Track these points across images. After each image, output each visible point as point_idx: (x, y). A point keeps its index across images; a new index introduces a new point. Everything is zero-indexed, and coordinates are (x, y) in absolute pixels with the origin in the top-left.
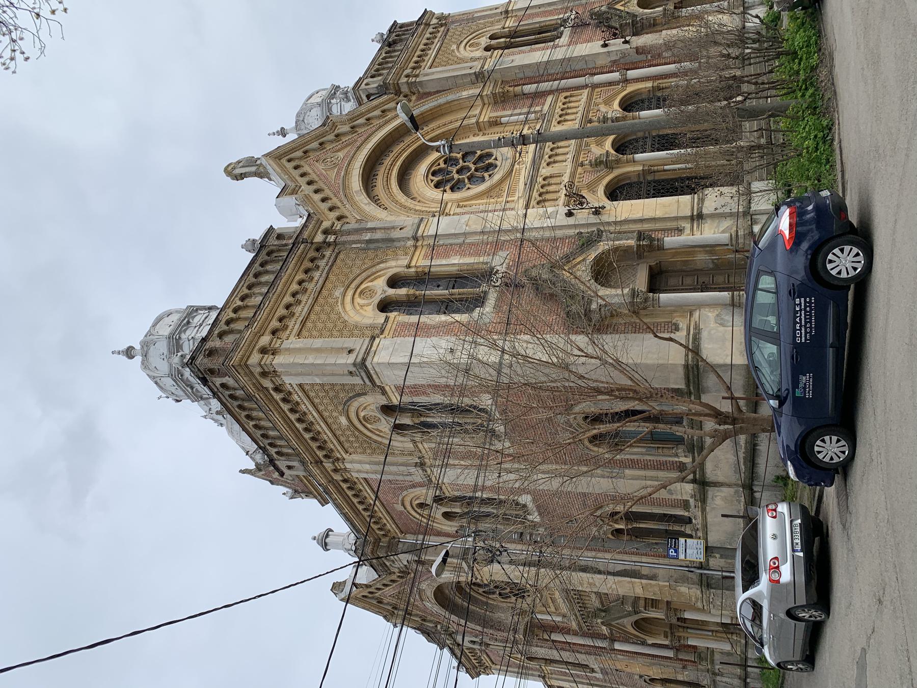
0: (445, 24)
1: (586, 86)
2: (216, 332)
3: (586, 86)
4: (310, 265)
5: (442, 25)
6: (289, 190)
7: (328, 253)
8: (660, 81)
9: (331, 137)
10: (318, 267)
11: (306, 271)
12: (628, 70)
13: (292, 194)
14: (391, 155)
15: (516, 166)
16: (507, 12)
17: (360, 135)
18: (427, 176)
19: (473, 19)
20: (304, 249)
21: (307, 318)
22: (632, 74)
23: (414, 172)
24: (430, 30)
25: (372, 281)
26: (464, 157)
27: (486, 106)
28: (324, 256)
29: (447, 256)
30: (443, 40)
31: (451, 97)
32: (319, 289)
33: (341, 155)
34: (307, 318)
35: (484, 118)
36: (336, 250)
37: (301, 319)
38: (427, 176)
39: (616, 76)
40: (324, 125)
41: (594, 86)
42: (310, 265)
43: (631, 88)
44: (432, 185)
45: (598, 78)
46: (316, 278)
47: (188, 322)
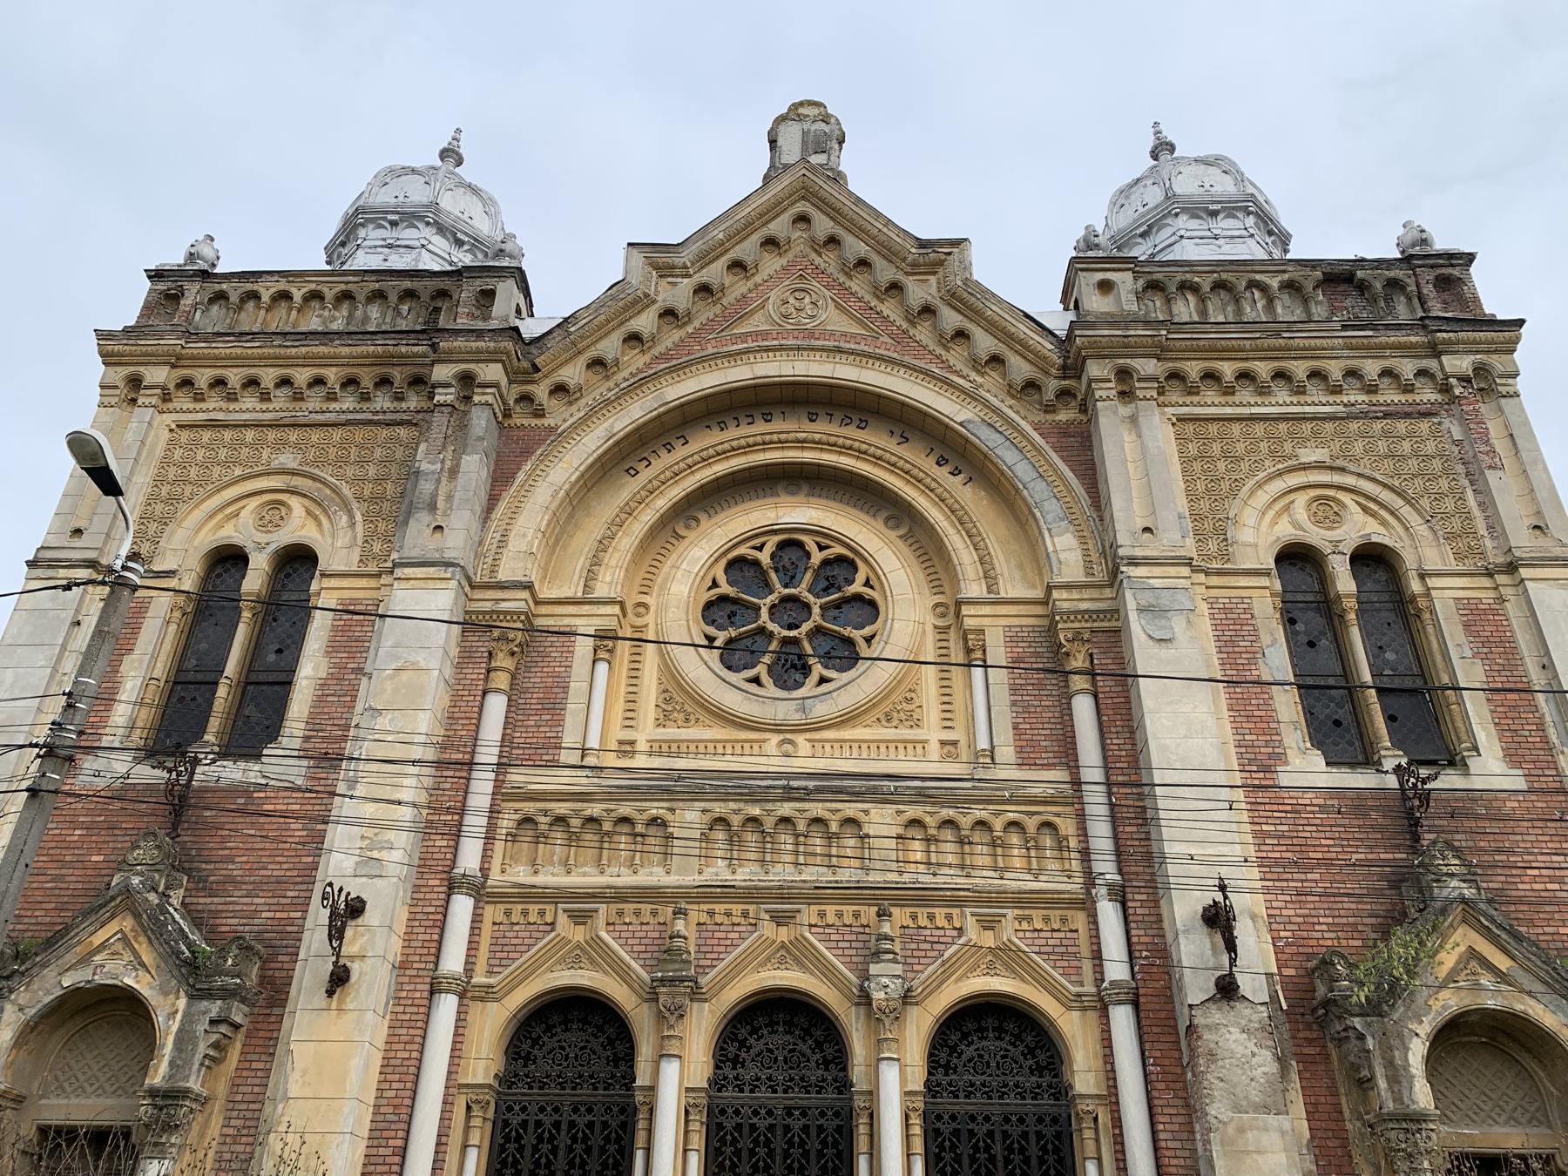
0: (1454, 400)
1: (1090, 879)
2: (224, 286)
3: (1090, 879)
4: (367, 382)
5: (1446, 389)
6: (662, 258)
7: (413, 402)
8: (1104, 1118)
9: (885, 272)
10: (399, 398)
11: (351, 382)
12: (1136, 1004)
13: (657, 267)
14: (851, 431)
15: (775, 739)
16: (1511, 568)
17: (902, 338)
18: (775, 532)
19: (1475, 478)
20: (416, 355)
21: (226, 426)
22: (1122, 1019)
23: (801, 498)
24: (1407, 368)
25: (308, 512)
26: (858, 598)
27: (1039, 610)
28: (402, 399)
29: (332, 649)
30: (1364, 415)
31: (1049, 510)
32: (302, 420)
33: (834, 320)
34: (226, 426)
35: (972, 617)
36: (420, 416)
37: (220, 416)
38: (775, 532)
39: (1117, 970)
40: (923, 244)
41: (1087, 905)
42: (367, 382)
43: (1073, 1028)
44: (742, 550)
45: (1109, 913)
46: (334, 406)
47: (394, 224)
